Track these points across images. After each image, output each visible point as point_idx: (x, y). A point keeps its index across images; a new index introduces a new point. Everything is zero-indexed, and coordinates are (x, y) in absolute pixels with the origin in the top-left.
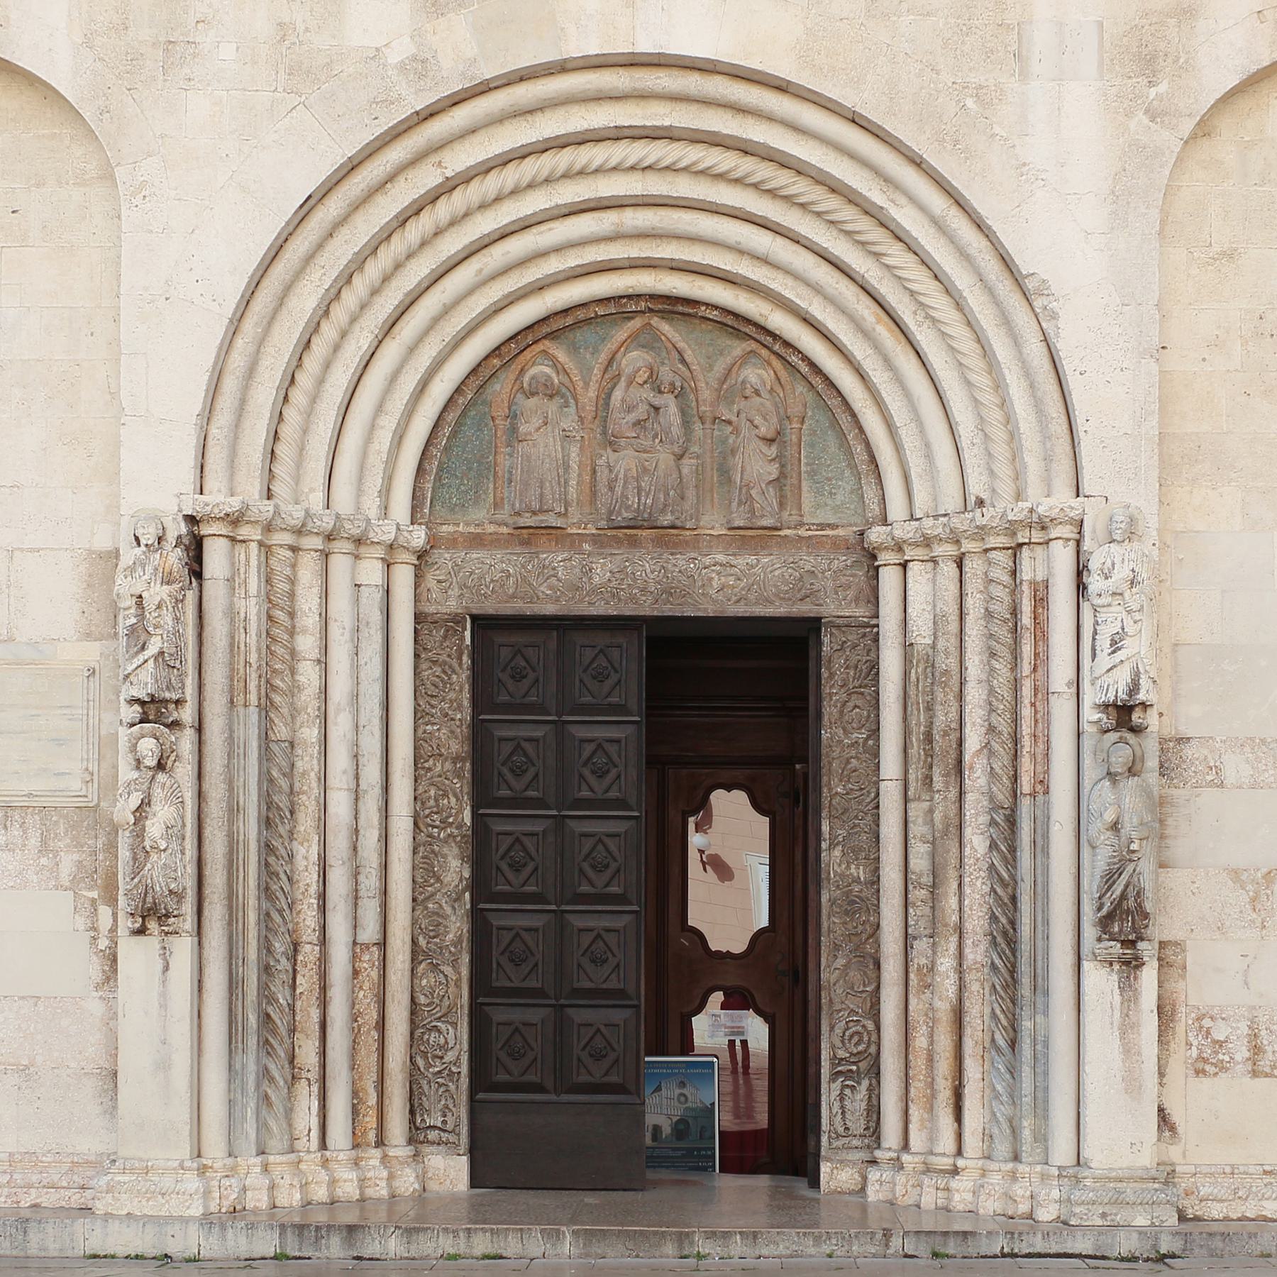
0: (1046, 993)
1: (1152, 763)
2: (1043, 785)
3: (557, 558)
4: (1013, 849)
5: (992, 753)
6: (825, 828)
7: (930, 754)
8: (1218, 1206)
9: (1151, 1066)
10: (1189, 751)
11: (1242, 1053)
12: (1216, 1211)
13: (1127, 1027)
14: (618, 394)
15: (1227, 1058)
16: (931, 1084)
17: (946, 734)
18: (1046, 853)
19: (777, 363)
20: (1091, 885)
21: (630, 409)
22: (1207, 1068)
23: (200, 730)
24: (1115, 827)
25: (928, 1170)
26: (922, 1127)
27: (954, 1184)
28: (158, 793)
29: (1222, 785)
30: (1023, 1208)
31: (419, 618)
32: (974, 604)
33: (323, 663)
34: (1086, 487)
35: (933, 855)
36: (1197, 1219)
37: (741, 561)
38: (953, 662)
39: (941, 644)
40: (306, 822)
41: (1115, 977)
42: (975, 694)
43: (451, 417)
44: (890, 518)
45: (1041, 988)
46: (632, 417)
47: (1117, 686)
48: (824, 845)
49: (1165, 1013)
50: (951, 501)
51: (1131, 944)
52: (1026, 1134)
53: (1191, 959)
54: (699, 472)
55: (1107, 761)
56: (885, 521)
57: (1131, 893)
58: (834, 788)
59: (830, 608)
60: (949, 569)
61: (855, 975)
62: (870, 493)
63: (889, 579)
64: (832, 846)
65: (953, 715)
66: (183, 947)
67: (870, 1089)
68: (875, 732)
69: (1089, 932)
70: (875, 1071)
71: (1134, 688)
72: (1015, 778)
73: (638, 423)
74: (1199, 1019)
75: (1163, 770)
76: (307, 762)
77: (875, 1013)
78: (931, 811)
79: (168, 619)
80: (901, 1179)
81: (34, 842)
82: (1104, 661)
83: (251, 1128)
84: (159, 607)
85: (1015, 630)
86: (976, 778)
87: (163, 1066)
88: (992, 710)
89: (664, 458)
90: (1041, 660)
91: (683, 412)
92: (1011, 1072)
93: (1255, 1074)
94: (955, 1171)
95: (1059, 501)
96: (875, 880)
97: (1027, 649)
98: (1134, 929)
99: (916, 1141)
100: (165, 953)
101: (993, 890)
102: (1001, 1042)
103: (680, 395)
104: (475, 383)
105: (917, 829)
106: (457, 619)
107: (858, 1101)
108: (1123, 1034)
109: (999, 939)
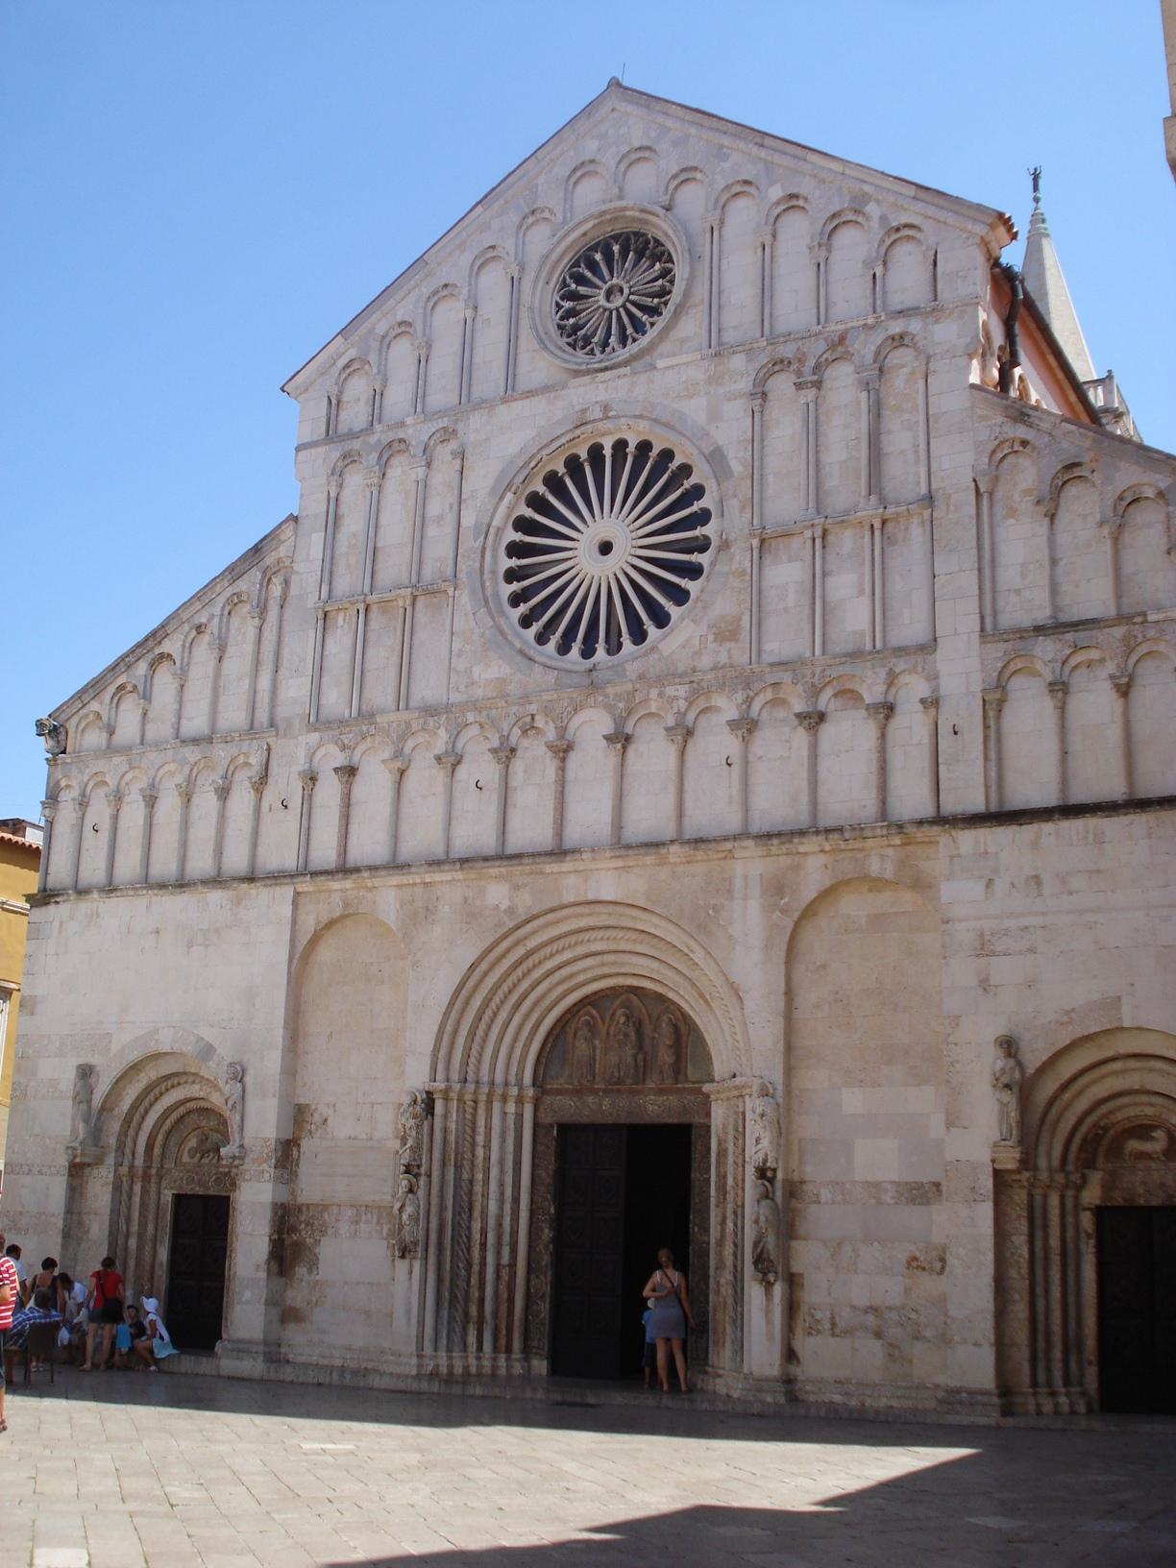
3: (590, 1099)
8: (814, 1396)
10: (805, 1187)
11: (827, 1326)
13: (768, 1312)
15: (821, 1328)
22: (813, 1332)
23: (429, 1176)
28: (407, 1202)
29: (819, 1203)
31: (536, 1125)
33: (487, 1146)
37: (662, 1099)
40: (477, 1214)
41: (763, 1289)
43: (551, 1040)
48: (691, 1226)
49: (792, 1308)
53: (806, 1282)
54: (645, 1060)
57: (765, 1251)
58: (695, 1199)
64: (695, 1225)
66: (417, 1265)
71: (765, 1161)
74: (809, 1309)
76: (478, 1188)
79: (414, 1133)
81: (375, 1220)
83: (444, 1341)
84: (410, 1128)
87: (408, 1312)
93: (833, 1335)
100: (411, 1266)
104: (560, 1024)
106: (551, 1126)
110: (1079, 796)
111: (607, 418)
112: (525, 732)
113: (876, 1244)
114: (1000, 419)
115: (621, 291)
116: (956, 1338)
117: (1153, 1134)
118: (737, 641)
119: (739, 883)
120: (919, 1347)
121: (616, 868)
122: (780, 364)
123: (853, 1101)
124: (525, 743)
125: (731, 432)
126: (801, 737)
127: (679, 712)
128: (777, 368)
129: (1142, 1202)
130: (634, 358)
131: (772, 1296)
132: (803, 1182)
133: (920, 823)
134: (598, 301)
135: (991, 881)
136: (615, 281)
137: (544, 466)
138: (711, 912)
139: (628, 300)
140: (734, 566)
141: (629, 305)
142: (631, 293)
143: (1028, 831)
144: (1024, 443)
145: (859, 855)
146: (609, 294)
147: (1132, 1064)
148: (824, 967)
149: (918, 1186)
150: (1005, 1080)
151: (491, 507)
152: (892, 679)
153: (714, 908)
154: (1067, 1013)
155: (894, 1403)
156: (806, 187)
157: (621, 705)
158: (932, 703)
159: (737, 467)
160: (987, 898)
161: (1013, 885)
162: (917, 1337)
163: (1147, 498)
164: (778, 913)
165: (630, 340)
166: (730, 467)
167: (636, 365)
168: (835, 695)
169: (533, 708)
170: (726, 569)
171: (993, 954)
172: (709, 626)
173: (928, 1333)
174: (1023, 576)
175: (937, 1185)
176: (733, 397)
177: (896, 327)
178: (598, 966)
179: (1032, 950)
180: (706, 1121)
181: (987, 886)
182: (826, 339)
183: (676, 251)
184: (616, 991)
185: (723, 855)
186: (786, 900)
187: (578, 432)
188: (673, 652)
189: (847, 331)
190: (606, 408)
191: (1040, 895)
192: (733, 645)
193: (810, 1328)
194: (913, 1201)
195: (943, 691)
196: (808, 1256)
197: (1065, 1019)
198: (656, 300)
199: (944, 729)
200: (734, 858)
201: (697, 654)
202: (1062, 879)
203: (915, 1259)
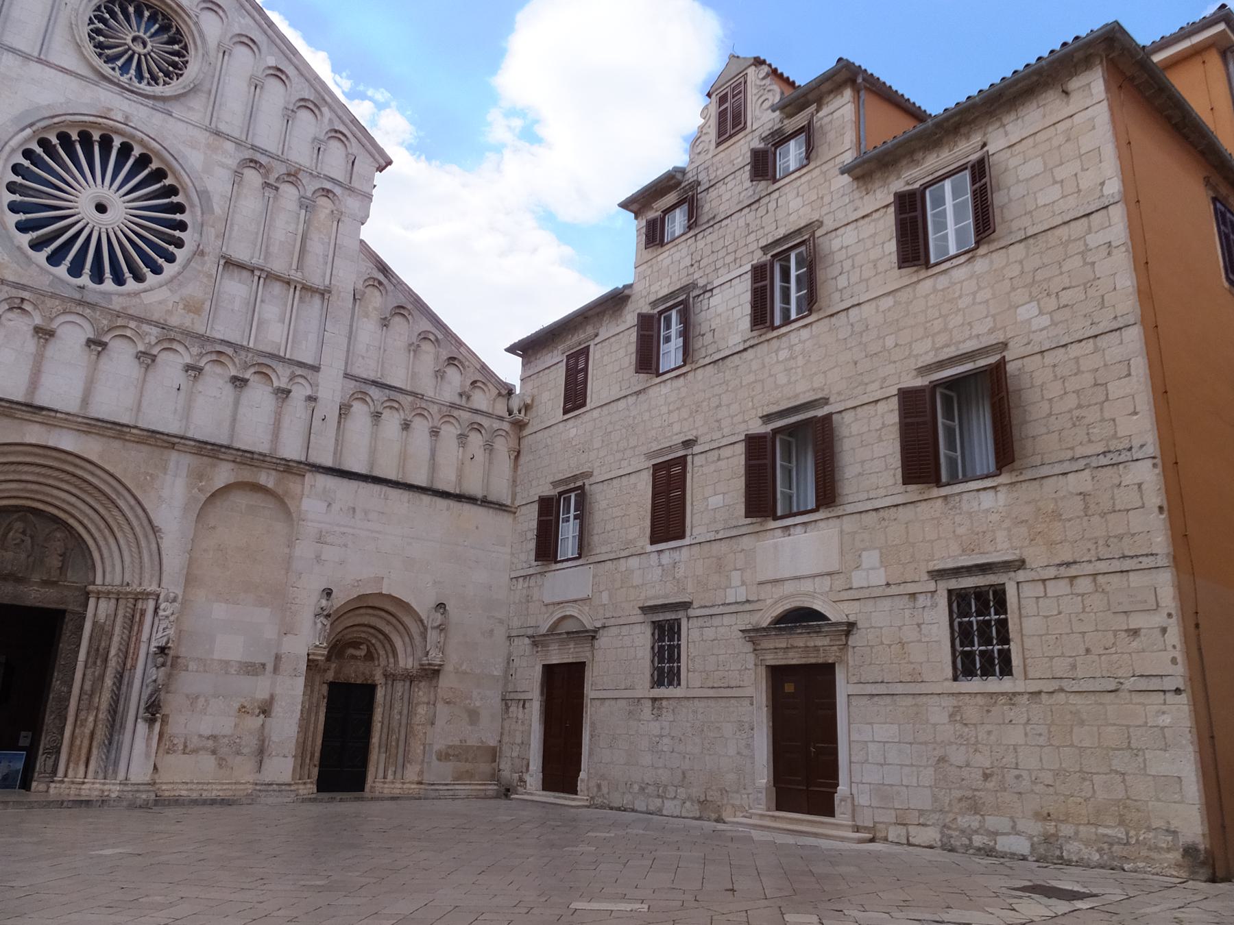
0: (125, 728)
1: (169, 663)
2: (134, 667)
4: (120, 684)
5: (119, 656)
6: (56, 674)
7: (97, 654)
9: (154, 750)
10: (179, 660)
11: (181, 747)
12: (167, 794)
13: (149, 739)
14: (11, 534)
16: (79, 756)
17: (104, 649)
18: (132, 687)
19: (67, 533)
20: (145, 697)
21: (14, 540)
24: (155, 681)
25: (73, 783)
26: (73, 770)
27: (84, 787)
30: (106, 794)
32: (121, 612)
34: (163, 585)
35: (92, 686)
36: (160, 796)
37: (43, 590)
38: (111, 628)
39: (107, 623)
42: (116, 639)
44: (97, 583)
45: (123, 727)
46: (15, 542)
47: (163, 643)
48: (54, 680)
49: (161, 735)
50: (118, 581)
51: (153, 715)
52: (111, 771)
55: (156, 662)
56: (94, 583)
59: (70, 607)
60: (113, 601)
61: (57, 721)
62: (91, 575)
63: (92, 602)
64: (57, 680)
65: (108, 643)
67: (56, 758)
68: (79, 646)
69: (141, 710)
70: (58, 752)
71: (167, 642)
72: (124, 664)
73: (15, 544)
75: (172, 666)
77: (62, 734)
78: (94, 672)
80: (63, 786)
82: (160, 634)
85: (132, 622)
86: (113, 663)
88: (121, 644)
89: (23, 556)
90: (140, 631)
91: (32, 542)
92: (108, 751)
93: (184, 753)
94: (83, 783)
95: (153, 588)
96: (70, 692)
97: (136, 628)
98: (156, 710)
99: (70, 773)
101: (112, 697)
102: (106, 742)
103: (32, 537)
105: (89, 676)
107: (50, 762)
108: (147, 740)
109: (112, 712)
110: (378, 473)
111: (127, 125)
112: (11, 309)
113: (221, 697)
114: (372, 266)
115: (145, 46)
116: (274, 754)
117: (361, 647)
118: (199, 315)
119: (172, 465)
120: (239, 758)
121: (79, 430)
122: (254, 163)
123: (220, 611)
124: (10, 315)
125: (218, 184)
126: (229, 388)
127: (149, 343)
128: (252, 165)
129: (353, 681)
130: (154, 98)
131: (153, 729)
132: (178, 657)
133: (300, 463)
134: (125, 39)
135: (329, 505)
136: (141, 34)
137: (62, 126)
138: (148, 478)
139: (149, 54)
140: (205, 269)
141: (149, 57)
142: (152, 50)
143: (354, 484)
144: (380, 283)
145: (255, 469)
146: (134, 39)
147: (371, 611)
148: (214, 528)
149: (253, 665)
150: (325, 613)
151: (12, 130)
152: (292, 378)
153: (151, 475)
154: (358, 581)
155: (220, 793)
156: (290, 71)
157: (105, 322)
158: (311, 399)
159: (218, 208)
160: (327, 513)
161: (341, 509)
162: (238, 753)
163: (430, 339)
164: (196, 490)
165: (146, 81)
166: (213, 207)
167: (159, 105)
168: (255, 373)
169: (26, 295)
170: (200, 268)
171: (326, 543)
172: (181, 299)
173: (245, 751)
174: (367, 351)
175: (264, 665)
176: (223, 166)
177: (328, 185)
178: (22, 490)
179: (345, 546)
180: (80, 609)
181: (328, 506)
182: (287, 167)
183: (196, 49)
184: (17, 509)
185: (166, 445)
186: (203, 483)
187: (100, 120)
188: (151, 303)
189: (300, 169)
190: (127, 117)
191: (353, 517)
192: (196, 316)
193: (169, 749)
194: (248, 673)
195: (319, 395)
196: (173, 704)
197: (356, 584)
198: (171, 69)
199: (318, 415)
200: (173, 448)
201: (169, 312)
202: (366, 512)
203: (244, 707)
